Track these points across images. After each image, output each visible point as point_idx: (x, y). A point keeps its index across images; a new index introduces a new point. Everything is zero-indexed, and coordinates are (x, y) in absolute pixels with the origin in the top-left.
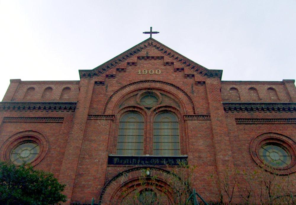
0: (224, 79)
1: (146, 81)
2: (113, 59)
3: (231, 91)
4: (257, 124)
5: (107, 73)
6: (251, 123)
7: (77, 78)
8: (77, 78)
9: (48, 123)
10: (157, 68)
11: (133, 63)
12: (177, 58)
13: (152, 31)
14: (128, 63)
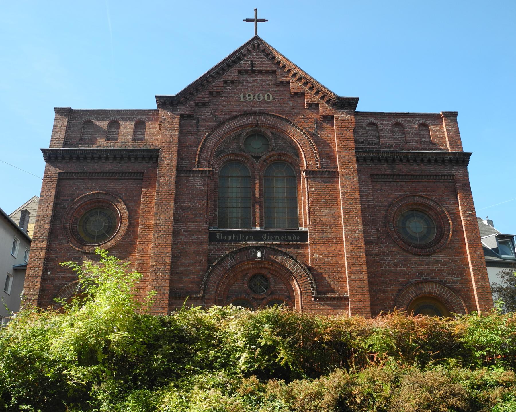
0: (359, 109)
1: (251, 114)
2: (203, 76)
3: (368, 128)
4: (398, 182)
5: (197, 99)
6: (391, 180)
7: (153, 106)
8: (153, 106)
9: (122, 181)
10: (267, 91)
11: (233, 82)
12: (295, 75)
13: (254, 23)
14: (225, 82)
